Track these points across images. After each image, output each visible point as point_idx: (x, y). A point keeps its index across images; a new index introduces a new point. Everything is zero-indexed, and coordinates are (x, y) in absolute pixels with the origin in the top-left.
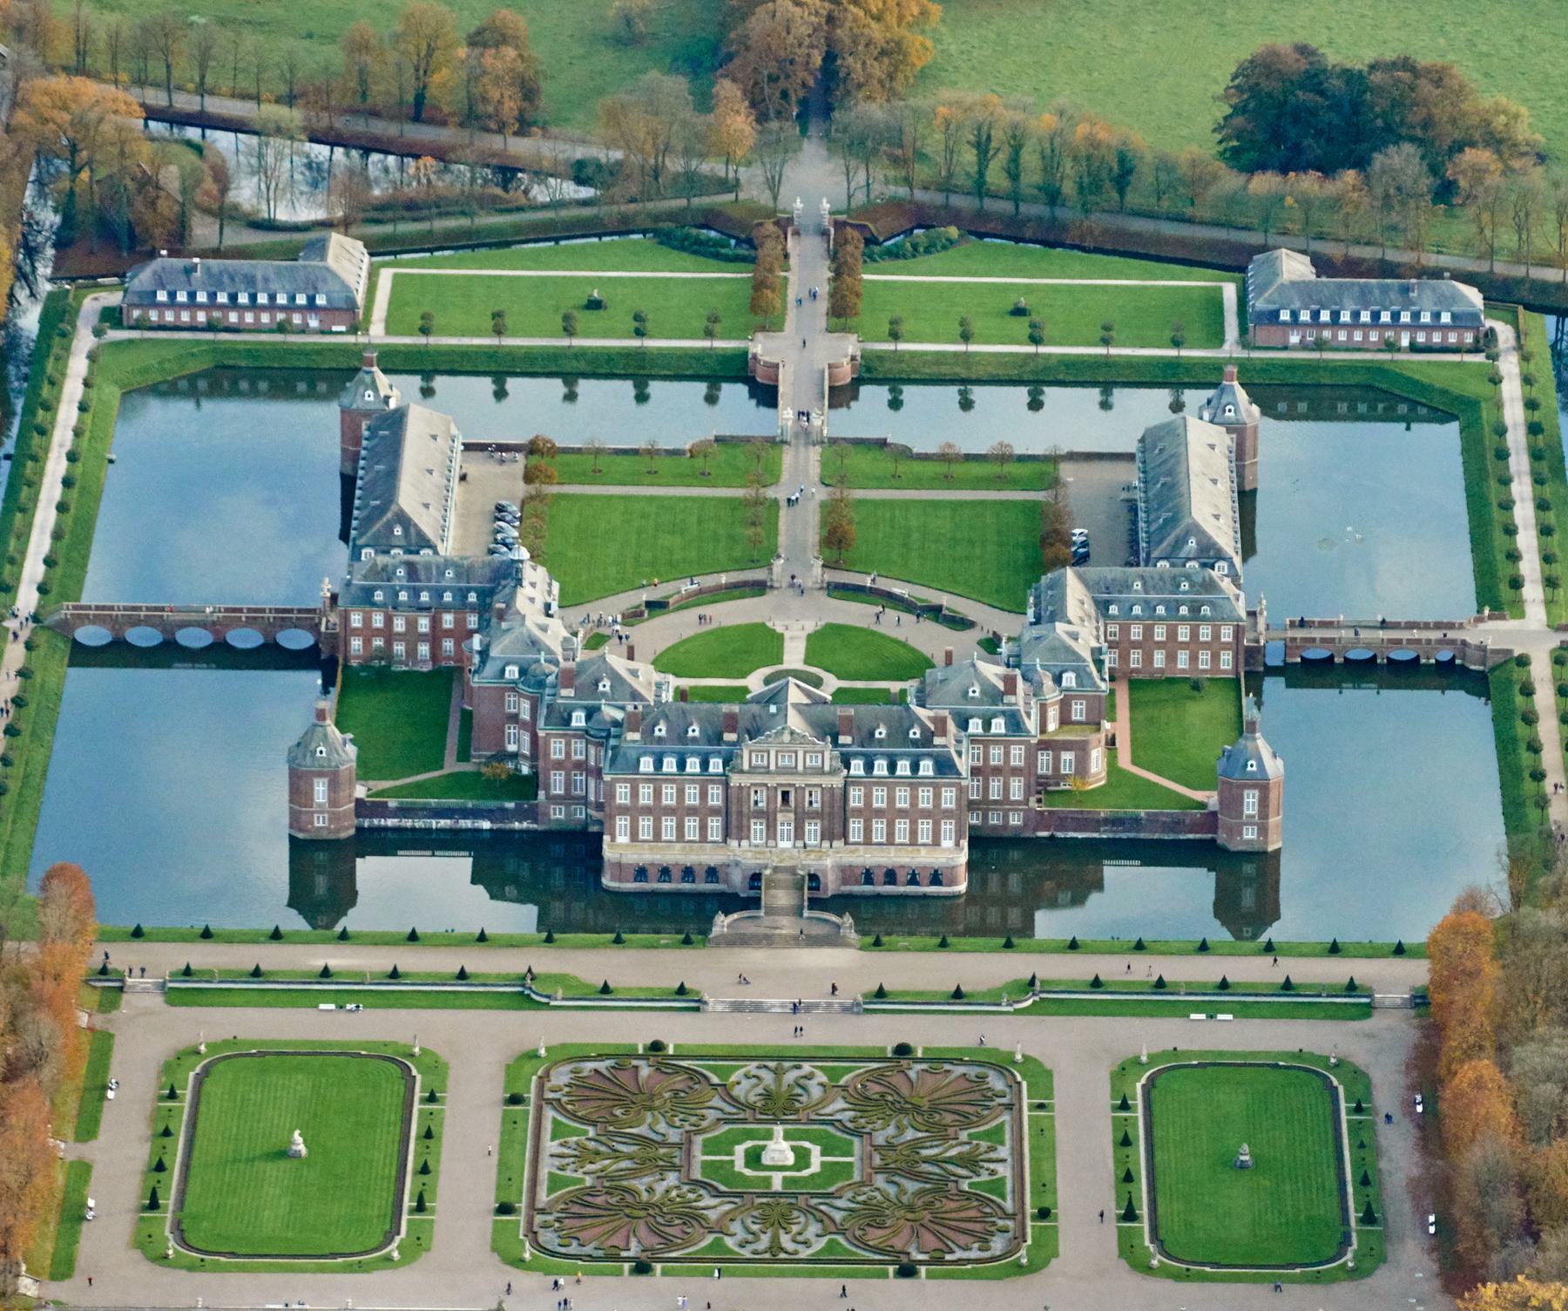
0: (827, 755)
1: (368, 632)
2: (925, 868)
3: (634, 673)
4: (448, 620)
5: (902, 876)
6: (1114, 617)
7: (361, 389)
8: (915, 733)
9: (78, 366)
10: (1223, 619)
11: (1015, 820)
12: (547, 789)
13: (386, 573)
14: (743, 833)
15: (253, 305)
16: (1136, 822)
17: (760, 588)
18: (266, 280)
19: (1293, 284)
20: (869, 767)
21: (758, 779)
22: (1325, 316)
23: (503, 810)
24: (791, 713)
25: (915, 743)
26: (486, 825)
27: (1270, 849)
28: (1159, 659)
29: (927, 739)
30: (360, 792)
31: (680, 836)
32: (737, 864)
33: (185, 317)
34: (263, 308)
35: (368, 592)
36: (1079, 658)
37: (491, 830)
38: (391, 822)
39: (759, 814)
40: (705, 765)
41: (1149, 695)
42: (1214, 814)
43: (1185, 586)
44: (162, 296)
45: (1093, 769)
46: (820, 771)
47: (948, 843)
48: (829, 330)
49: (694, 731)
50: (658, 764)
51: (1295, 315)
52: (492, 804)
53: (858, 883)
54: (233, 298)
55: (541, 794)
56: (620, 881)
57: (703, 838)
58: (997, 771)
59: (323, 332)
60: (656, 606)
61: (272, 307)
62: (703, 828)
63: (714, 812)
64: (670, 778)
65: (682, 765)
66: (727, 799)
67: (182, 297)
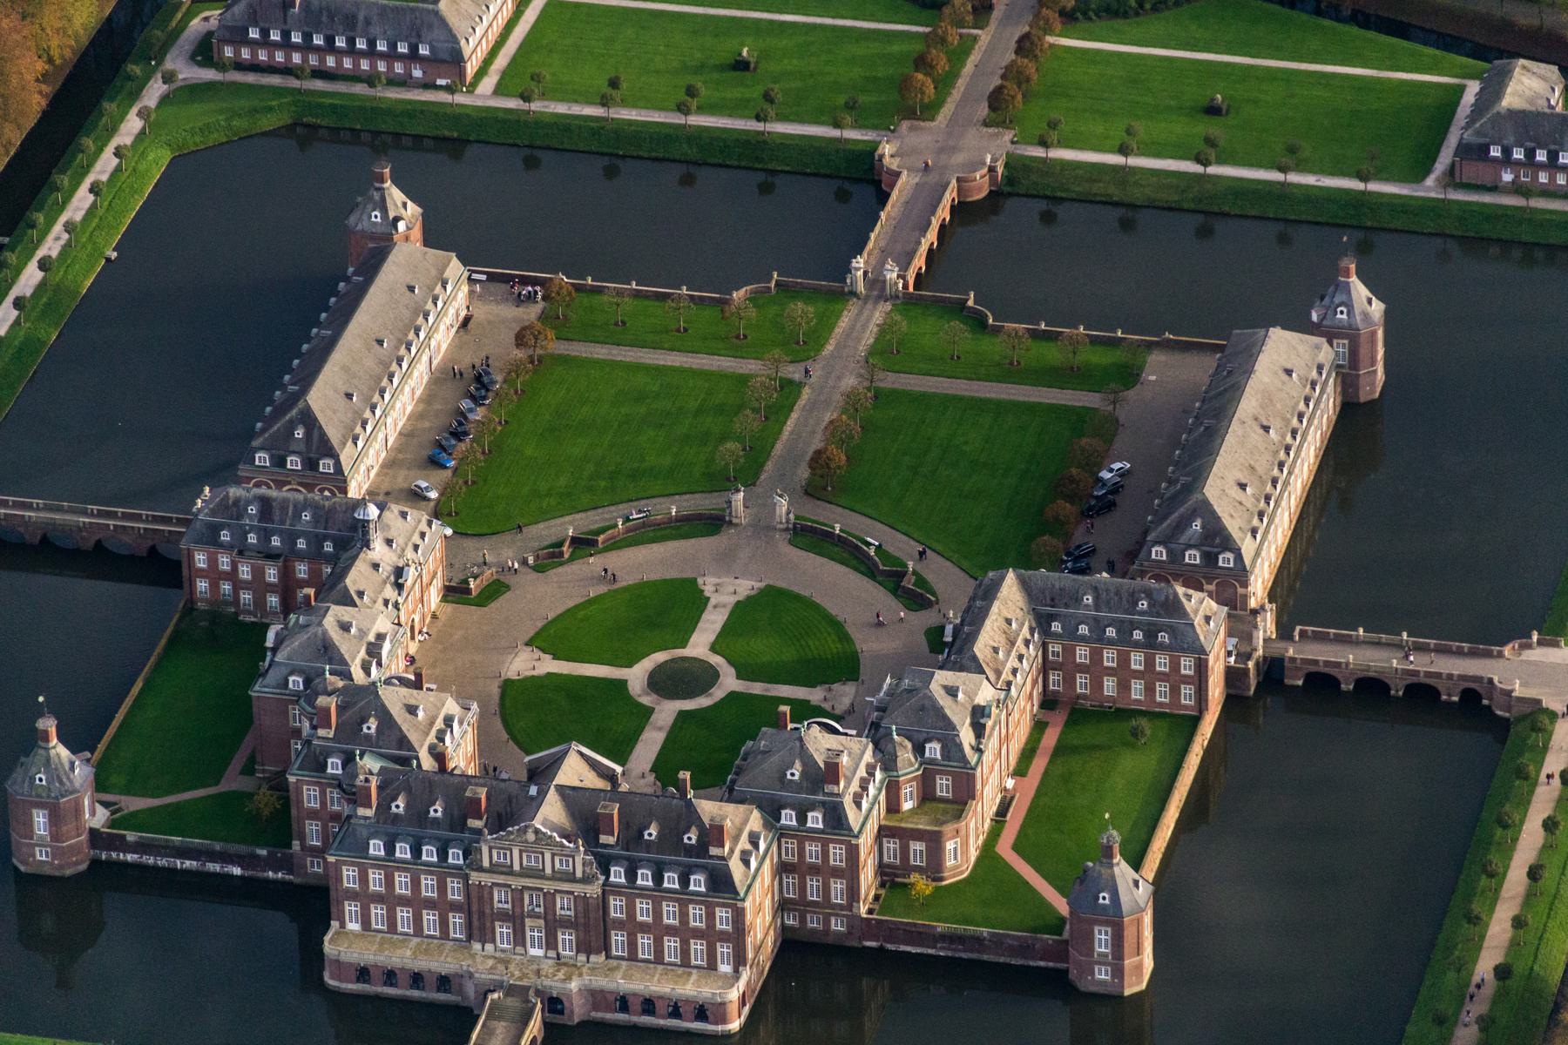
0: (579, 860)
1: (214, 575)
2: (687, 1001)
3: (412, 710)
4: (302, 570)
5: (661, 1007)
6: (1057, 636)
7: (370, 206)
8: (692, 837)
9: (132, 124)
10: (1183, 650)
11: (837, 926)
12: (302, 837)
13: (234, 510)
14: (487, 936)
15: (351, 50)
16: (977, 941)
17: (714, 523)
18: (368, 22)
19: (1513, 114)
20: (631, 875)
21: (500, 879)
22: (1541, 156)
23: (258, 856)
24: (552, 796)
25: (689, 851)
26: (237, 871)
27: (1127, 992)
28: (1109, 686)
29: (701, 849)
30: (98, 818)
31: (418, 931)
32: (471, 975)
33: (279, 57)
34: (362, 54)
35: (214, 529)
36: (950, 726)
37: (241, 878)
38: (130, 857)
39: (504, 916)
40: (443, 855)
41: (1089, 733)
42: (1066, 942)
43: (1143, 605)
44: (254, 34)
45: (950, 862)
46: (571, 878)
47: (725, 968)
48: (986, 124)
49: (437, 811)
50: (390, 849)
51: (1507, 152)
52: (242, 849)
53: (608, 1009)
54: (330, 40)
55: (296, 845)
56: (340, 980)
57: (445, 935)
58: (814, 870)
59: (429, 86)
60: (584, 544)
61: (371, 53)
62: (444, 924)
63: (455, 907)
64: (402, 865)
65: (417, 852)
66: (468, 895)
67: (275, 36)
